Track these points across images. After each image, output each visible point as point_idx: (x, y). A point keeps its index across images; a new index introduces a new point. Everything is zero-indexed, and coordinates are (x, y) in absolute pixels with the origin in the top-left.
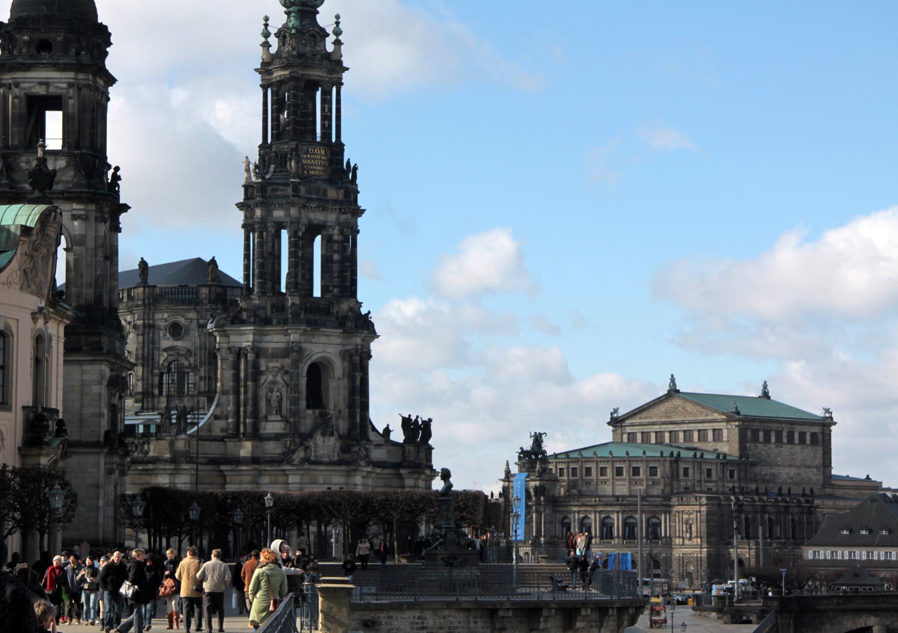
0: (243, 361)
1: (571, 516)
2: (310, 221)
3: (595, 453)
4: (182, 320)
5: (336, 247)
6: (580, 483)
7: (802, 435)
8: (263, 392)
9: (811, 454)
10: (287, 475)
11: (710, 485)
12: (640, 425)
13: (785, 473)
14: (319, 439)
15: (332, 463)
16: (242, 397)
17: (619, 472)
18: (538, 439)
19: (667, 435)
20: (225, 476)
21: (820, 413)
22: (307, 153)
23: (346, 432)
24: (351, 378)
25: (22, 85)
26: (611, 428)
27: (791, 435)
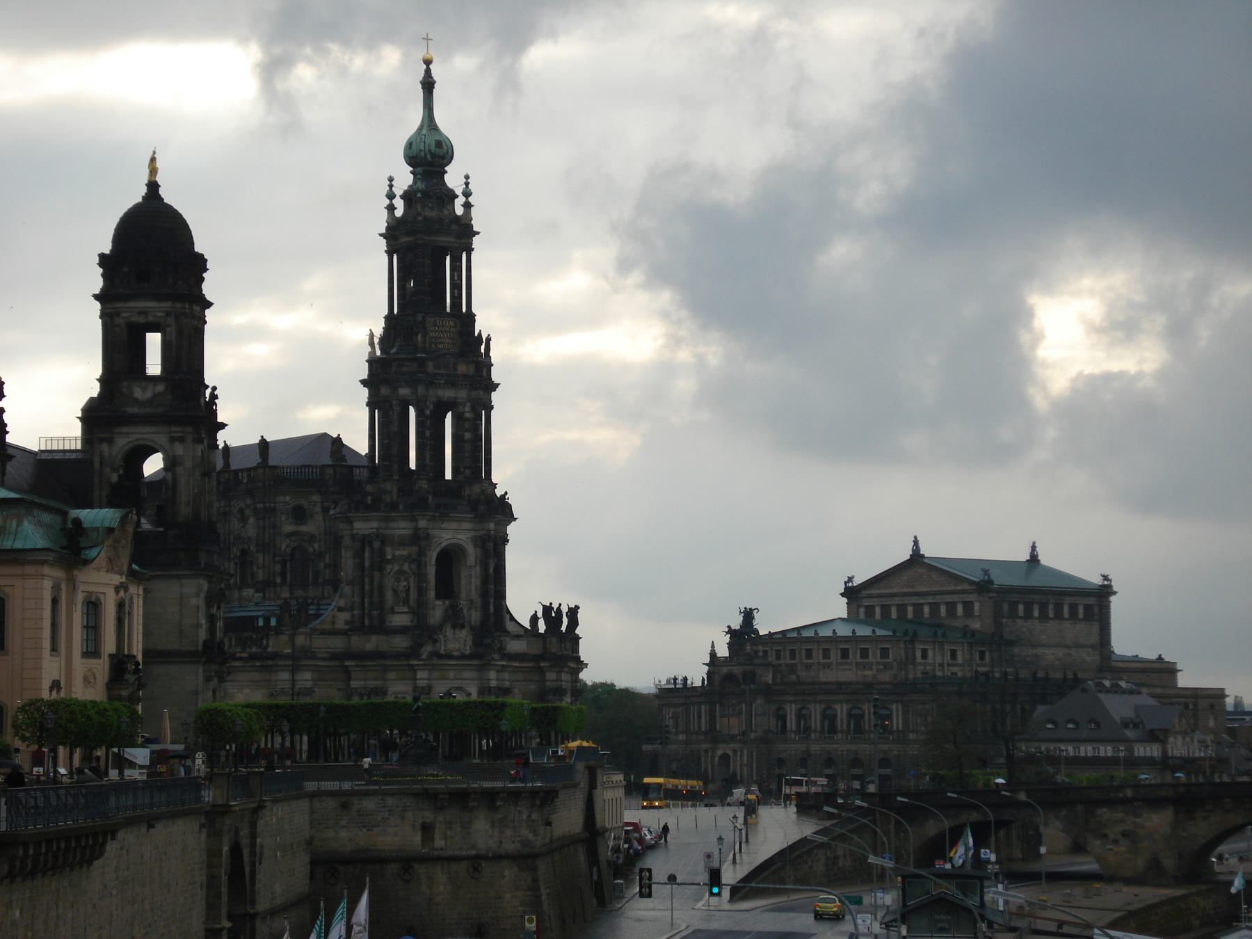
0: (367, 549)
1: (787, 707)
3: (816, 633)
4: (304, 503)
5: (467, 425)
6: (799, 667)
7: (1074, 608)
8: (389, 582)
10: (415, 671)
11: (955, 669)
12: (880, 596)
13: (1050, 655)
14: (448, 631)
15: (463, 657)
16: (367, 587)
17: (845, 654)
18: (748, 615)
19: (910, 609)
20: (349, 672)
22: (435, 325)
24: (485, 566)
25: (123, 315)
26: (845, 600)
27: (1058, 608)
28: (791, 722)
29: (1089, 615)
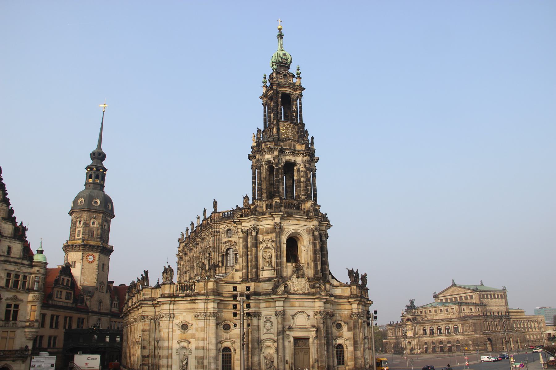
1: (426, 327)
5: (302, 174)
7: (498, 295)
8: (260, 255)
10: (275, 301)
13: (495, 309)
16: (249, 257)
18: (412, 302)
19: (453, 299)
21: (501, 289)
23: (313, 276)
27: (494, 295)
29: (502, 297)
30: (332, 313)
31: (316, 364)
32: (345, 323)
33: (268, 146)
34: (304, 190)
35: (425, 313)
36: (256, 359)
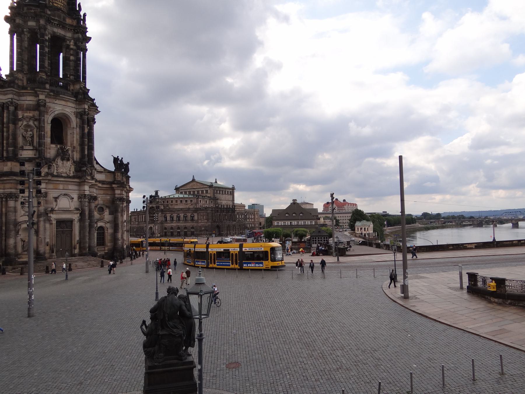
2: (54, 32)
5: (72, 52)
7: (228, 192)
8: (20, 132)
9: (230, 197)
13: (224, 202)
15: (68, 177)
16: (5, 134)
17: (181, 201)
18: (157, 192)
21: (231, 187)
23: (78, 160)
24: (82, 128)
27: (225, 192)
28: (168, 218)
30: (96, 197)
31: (78, 245)
32: (107, 207)
33: (33, 11)
34: (73, 70)
35: (168, 202)
36: (11, 241)
